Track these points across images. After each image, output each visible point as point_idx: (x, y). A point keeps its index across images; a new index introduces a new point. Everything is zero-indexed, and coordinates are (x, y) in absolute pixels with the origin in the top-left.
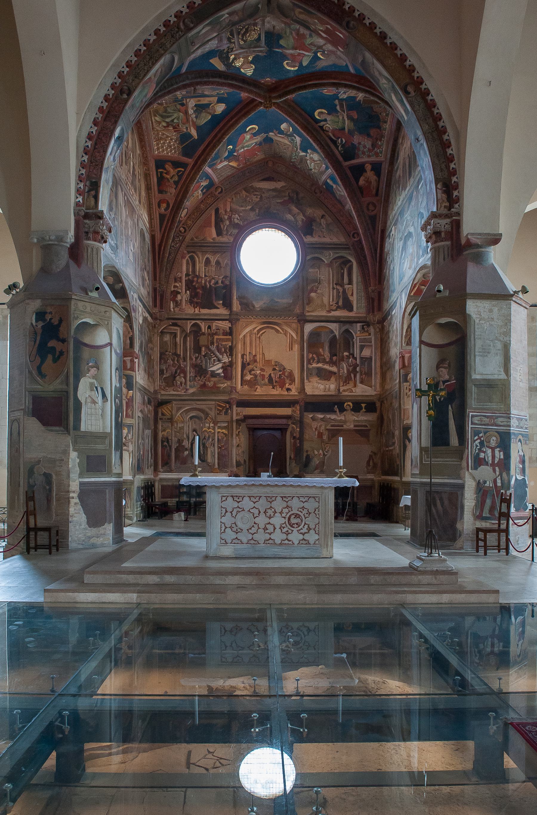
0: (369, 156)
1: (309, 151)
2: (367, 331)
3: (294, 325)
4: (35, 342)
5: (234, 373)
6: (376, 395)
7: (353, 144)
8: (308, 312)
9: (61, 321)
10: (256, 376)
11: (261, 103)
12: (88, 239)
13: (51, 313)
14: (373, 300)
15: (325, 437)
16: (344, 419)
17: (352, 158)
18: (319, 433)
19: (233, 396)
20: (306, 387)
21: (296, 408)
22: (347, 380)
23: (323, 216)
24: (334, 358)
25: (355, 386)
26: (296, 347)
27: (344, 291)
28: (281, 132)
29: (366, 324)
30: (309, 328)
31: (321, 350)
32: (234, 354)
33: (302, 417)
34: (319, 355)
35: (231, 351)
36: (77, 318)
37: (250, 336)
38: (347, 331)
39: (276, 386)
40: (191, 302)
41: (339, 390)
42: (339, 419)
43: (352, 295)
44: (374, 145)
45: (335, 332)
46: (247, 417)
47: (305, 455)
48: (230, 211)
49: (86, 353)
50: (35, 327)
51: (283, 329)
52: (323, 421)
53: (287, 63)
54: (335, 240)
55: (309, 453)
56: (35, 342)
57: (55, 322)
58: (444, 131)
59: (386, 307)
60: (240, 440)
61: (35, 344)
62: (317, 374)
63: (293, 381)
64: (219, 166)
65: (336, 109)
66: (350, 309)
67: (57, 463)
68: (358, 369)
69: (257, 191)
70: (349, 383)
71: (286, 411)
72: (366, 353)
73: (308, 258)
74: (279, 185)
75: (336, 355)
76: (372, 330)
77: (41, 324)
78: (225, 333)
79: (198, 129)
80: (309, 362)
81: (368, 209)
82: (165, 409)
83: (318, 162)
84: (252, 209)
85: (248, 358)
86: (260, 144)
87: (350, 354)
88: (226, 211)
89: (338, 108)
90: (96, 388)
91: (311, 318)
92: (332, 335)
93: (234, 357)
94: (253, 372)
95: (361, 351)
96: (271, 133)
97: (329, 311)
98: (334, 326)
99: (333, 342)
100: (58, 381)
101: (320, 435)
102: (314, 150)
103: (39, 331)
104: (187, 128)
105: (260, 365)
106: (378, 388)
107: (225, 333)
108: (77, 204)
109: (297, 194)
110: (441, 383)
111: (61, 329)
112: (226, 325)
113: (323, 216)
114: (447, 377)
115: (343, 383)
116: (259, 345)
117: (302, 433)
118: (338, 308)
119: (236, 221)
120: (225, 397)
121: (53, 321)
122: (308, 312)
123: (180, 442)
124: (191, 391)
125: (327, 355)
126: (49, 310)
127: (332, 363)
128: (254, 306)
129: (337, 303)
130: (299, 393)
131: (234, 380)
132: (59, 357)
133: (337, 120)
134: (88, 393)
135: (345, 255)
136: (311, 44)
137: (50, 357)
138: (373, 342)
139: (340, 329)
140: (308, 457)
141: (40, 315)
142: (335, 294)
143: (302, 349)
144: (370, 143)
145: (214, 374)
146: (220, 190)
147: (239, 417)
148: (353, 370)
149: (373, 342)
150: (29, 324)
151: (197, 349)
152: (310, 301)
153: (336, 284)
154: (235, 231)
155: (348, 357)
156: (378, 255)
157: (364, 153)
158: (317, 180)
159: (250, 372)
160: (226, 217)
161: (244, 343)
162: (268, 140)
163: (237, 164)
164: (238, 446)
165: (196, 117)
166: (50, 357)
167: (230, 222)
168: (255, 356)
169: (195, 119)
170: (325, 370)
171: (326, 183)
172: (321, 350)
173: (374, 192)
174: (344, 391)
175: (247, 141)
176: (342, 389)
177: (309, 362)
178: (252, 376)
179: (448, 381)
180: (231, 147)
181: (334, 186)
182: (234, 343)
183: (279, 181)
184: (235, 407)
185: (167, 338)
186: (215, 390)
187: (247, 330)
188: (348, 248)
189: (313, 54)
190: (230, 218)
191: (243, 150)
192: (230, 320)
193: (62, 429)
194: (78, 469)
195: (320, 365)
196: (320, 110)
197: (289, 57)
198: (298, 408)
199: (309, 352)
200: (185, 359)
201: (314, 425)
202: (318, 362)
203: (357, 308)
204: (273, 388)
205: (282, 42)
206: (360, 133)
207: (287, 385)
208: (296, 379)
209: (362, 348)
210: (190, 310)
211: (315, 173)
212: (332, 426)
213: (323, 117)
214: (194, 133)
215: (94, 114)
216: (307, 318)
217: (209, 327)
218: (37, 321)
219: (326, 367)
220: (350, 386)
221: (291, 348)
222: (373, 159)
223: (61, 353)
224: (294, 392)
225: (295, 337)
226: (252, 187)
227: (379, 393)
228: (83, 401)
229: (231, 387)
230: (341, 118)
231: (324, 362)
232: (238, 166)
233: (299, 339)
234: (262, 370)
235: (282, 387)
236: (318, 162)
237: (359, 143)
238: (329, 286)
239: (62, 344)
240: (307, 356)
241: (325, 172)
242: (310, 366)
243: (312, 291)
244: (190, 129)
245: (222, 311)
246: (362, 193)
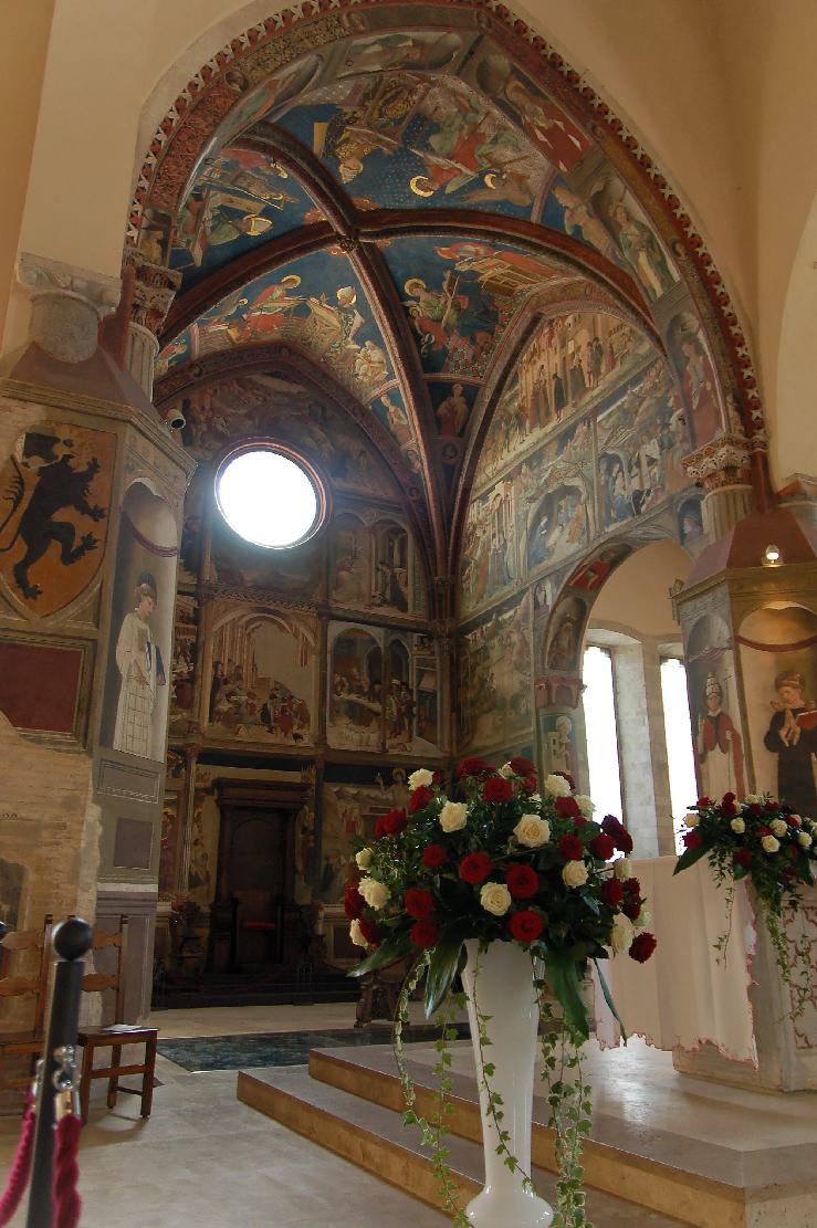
0: (463, 373)
1: (367, 343)
2: (429, 648)
3: (311, 622)
4: (17, 502)
5: (197, 695)
6: (445, 758)
7: (444, 348)
8: (336, 601)
9: (94, 466)
10: (238, 705)
11: (340, 237)
12: (138, 321)
13: (69, 443)
14: (440, 595)
15: (360, 832)
16: (391, 798)
17: (435, 370)
18: (348, 822)
19: (195, 740)
20: (328, 735)
21: (310, 772)
22: (397, 729)
23: (362, 452)
24: (377, 687)
25: (410, 739)
26: (313, 660)
27: (394, 576)
28: (333, 301)
29: (428, 636)
30: (336, 629)
31: (355, 670)
32: (201, 658)
33: (319, 791)
34: (350, 678)
36: (131, 470)
37: (233, 630)
38: (397, 643)
39: (276, 728)
41: (384, 744)
42: (384, 797)
43: (406, 584)
44: (475, 358)
45: (378, 640)
46: (219, 784)
47: (323, 864)
48: (211, 409)
50: (22, 468)
51: (291, 626)
52: (358, 801)
53: (418, 181)
54: (380, 493)
55: (331, 861)
56: (17, 502)
57: (80, 465)
59: (471, 607)
60: (200, 831)
61: (14, 510)
62: (347, 713)
63: (305, 720)
64: (213, 329)
65: (442, 286)
66: (404, 608)
67: (46, 835)
69: (257, 389)
70: (400, 734)
71: (294, 777)
72: (428, 684)
73: (338, 512)
74: (295, 389)
75: (380, 683)
77: (37, 463)
79: (208, 249)
80: (335, 690)
81: (444, 454)
83: (377, 365)
84: (249, 416)
85: (226, 670)
86: (286, 313)
87: (403, 683)
88: (203, 408)
89: (445, 285)
90: (149, 644)
91: (340, 613)
92: (373, 647)
93: (199, 664)
94: (233, 698)
96: (313, 299)
97: (371, 606)
98: (376, 633)
99: (375, 659)
100: (73, 610)
101: (352, 827)
102: (379, 343)
103: (32, 480)
104: (189, 241)
105: (247, 686)
106: (447, 748)
109: (324, 409)
110: (790, 713)
111: (92, 485)
113: (362, 452)
114: (800, 703)
115: (391, 733)
116: (248, 651)
117: (319, 820)
118: (385, 602)
119: (220, 428)
121: (71, 462)
122: (336, 601)
125: (365, 681)
126: (64, 434)
127: (375, 697)
128: (242, 578)
129: (383, 594)
130: (316, 744)
131: (196, 710)
132: (81, 552)
133: (435, 304)
134: (135, 654)
135: (395, 520)
136: (486, 156)
137: (55, 548)
138: (438, 666)
139: (386, 637)
140: (328, 867)
141: (38, 443)
142: (380, 579)
144: (471, 352)
146: (197, 371)
147: (202, 785)
148: (407, 711)
149: (438, 666)
150: (6, 458)
152: (338, 584)
153: (381, 563)
154: (218, 445)
155: (399, 688)
156: (453, 528)
157: (457, 366)
158: (361, 395)
159: (228, 696)
160: (203, 418)
161: (221, 641)
162: (303, 311)
163: (238, 334)
164: (196, 843)
165: (213, 229)
166: (55, 548)
167: (209, 427)
168: (239, 667)
169: (209, 231)
170: (362, 706)
171: (377, 401)
172: (355, 670)
173: (458, 431)
174: (392, 747)
175: (273, 301)
176: (389, 743)
177: (335, 690)
178: (231, 705)
179: (802, 710)
180: (246, 301)
181: (392, 409)
182: (202, 639)
183: (295, 382)
187: (228, 618)
188: (401, 509)
189: (476, 176)
190: (209, 421)
191: (258, 313)
193: (68, 737)
194: (97, 854)
195: (353, 697)
196: (415, 280)
197: (429, 170)
198: (314, 772)
199: (334, 672)
201: (341, 806)
202: (350, 691)
203: (414, 606)
204: (270, 731)
205: (434, 141)
206: (462, 334)
207: (295, 727)
208: (312, 718)
209: (421, 674)
211: (362, 382)
212: (372, 810)
213: (418, 292)
214: (198, 254)
216: (334, 612)
218: (27, 453)
219: (364, 701)
220: (402, 738)
221: (304, 662)
222: (469, 378)
223: (89, 543)
224: (307, 741)
225: (313, 644)
226: (250, 381)
227: (447, 755)
228: (124, 672)
229: (190, 722)
230: (442, 302)
231: (360, 691)
232: (237, 339)
233: (319, 647)
234: (249, 694)
236: (377, 365)
237: (455, 349)
238: (371, 567)
239: (88, 519)
240: (332, 678)
241: (382, 383)
242: (336, 698)
243: (342, 568)
244: (194, 245)
246: (439, 426)
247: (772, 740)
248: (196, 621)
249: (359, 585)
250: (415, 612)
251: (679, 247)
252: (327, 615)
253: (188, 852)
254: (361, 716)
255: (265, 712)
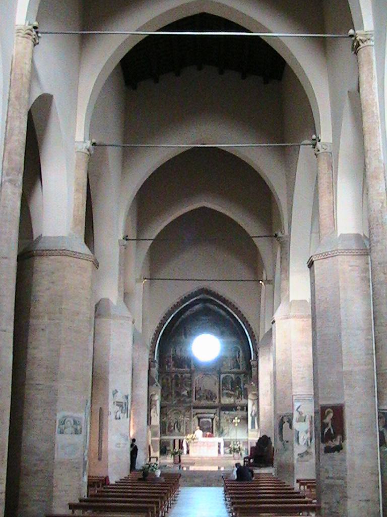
19: (192, 404)
25: (242, 399)
29: (246, 374)
30: (222, 376)
35: (191, 385)
38: (238, 377)
40: (174, 366)
49: (153, 402)
58: (254, 336)
66: (239, 368)
68: (243, 393)
76: (248, 377)
78: (188, 378)
82: (164, 409)
85: (198, 389)
95: (244, 384)
98: (233, 376)
99: (232, 382)
107: (188, 378)
108: (149, 359)
112: (189, 375)
117: (220, 419)
120: (189, 405)
123: (170, 423)
124: (174, 402)
127: (232, 390)
143: (220, 385)
145: (183, 395)
148: (240, 393)
151: (177, 385)
176: (236, 401)
184: (192, 409)
185: (165, 380)
186: (184, 402)
192: (190, 373)
195: (227, 391)
200: (172, 389)
201: (225, 416)
210: (174, 369)
215: (154, 332)
217: (182, 376)
220: (240, 399)
221: (215, 384)
231: (229, 389)
235: (212, 400)
245: (187, 369)
247: (251, 414)
248: (190, 379)
249: (229, 365)
250: (242, 368)
251: (245, 323)
252: (220, 373)
253: (192, 427)
254: (229, 396)
255: (207, 398)
